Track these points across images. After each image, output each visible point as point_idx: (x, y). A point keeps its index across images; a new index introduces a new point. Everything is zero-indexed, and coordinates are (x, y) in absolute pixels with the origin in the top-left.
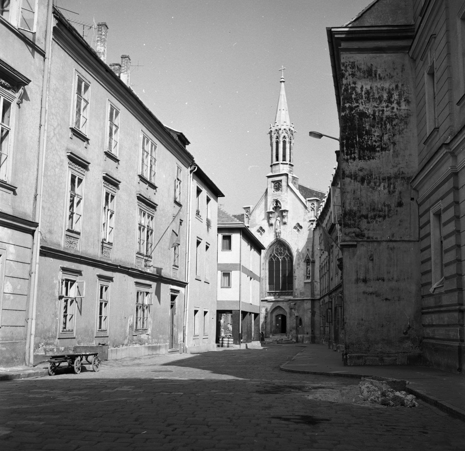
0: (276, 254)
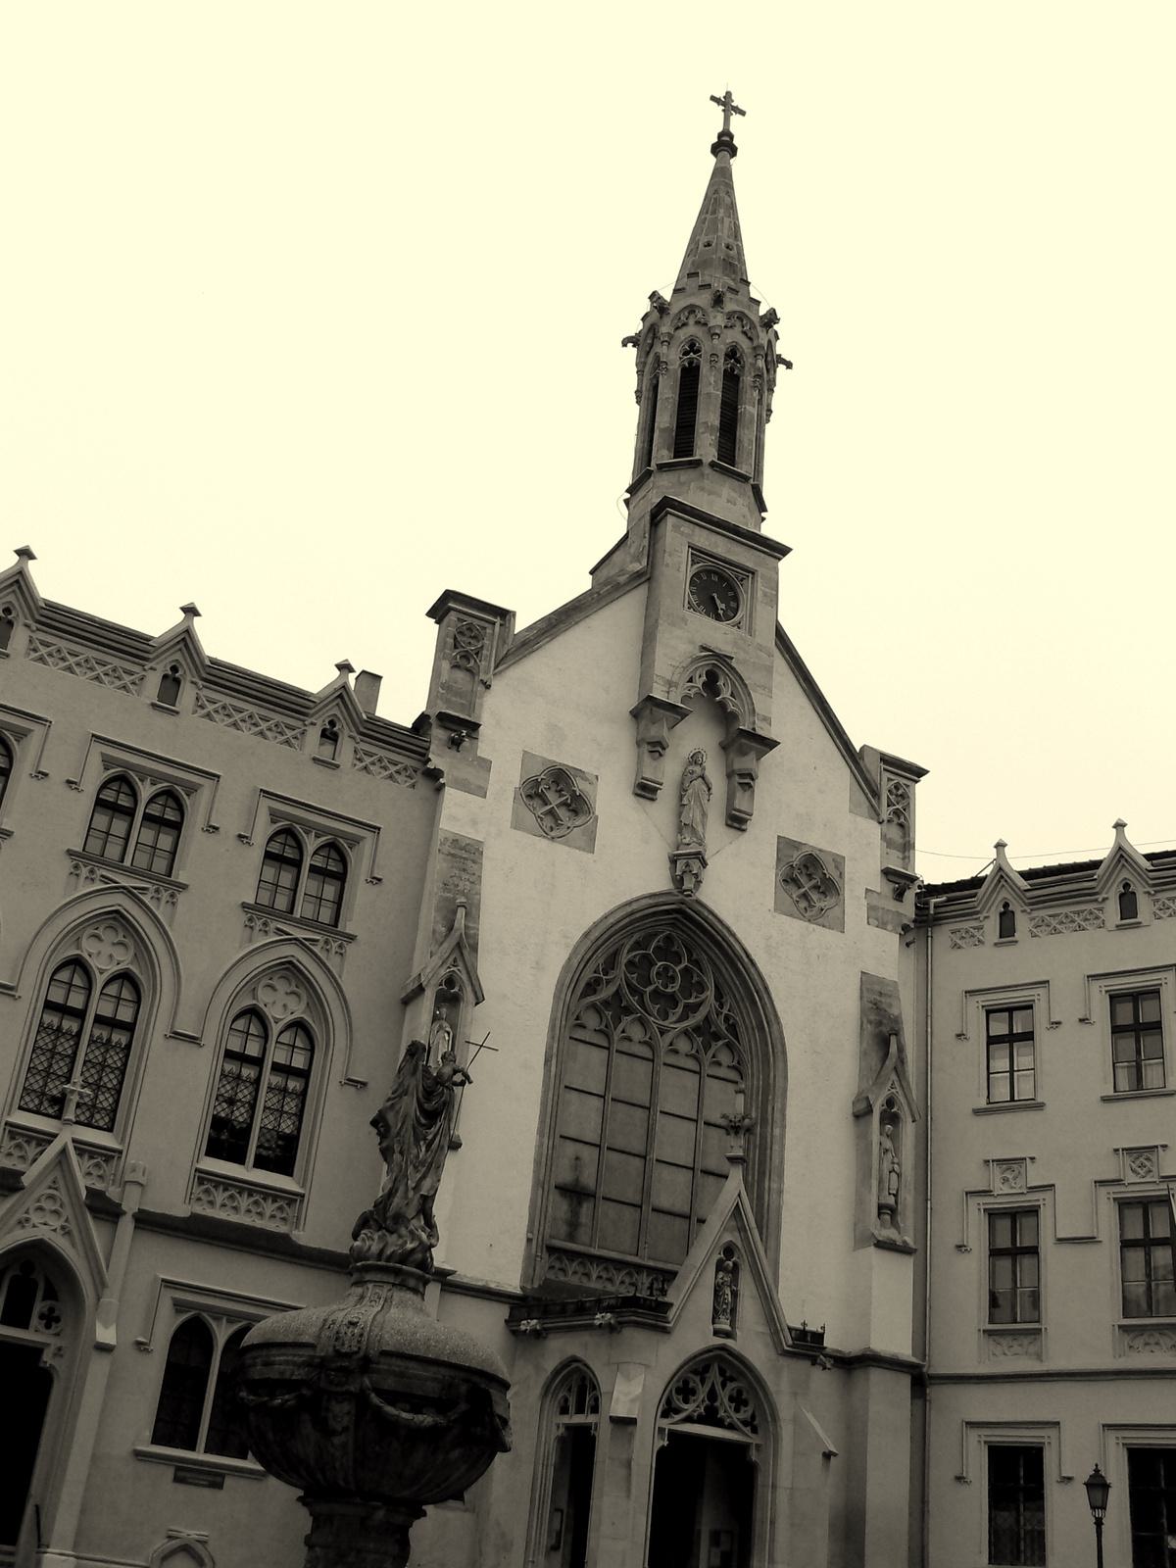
0: (634, 991)
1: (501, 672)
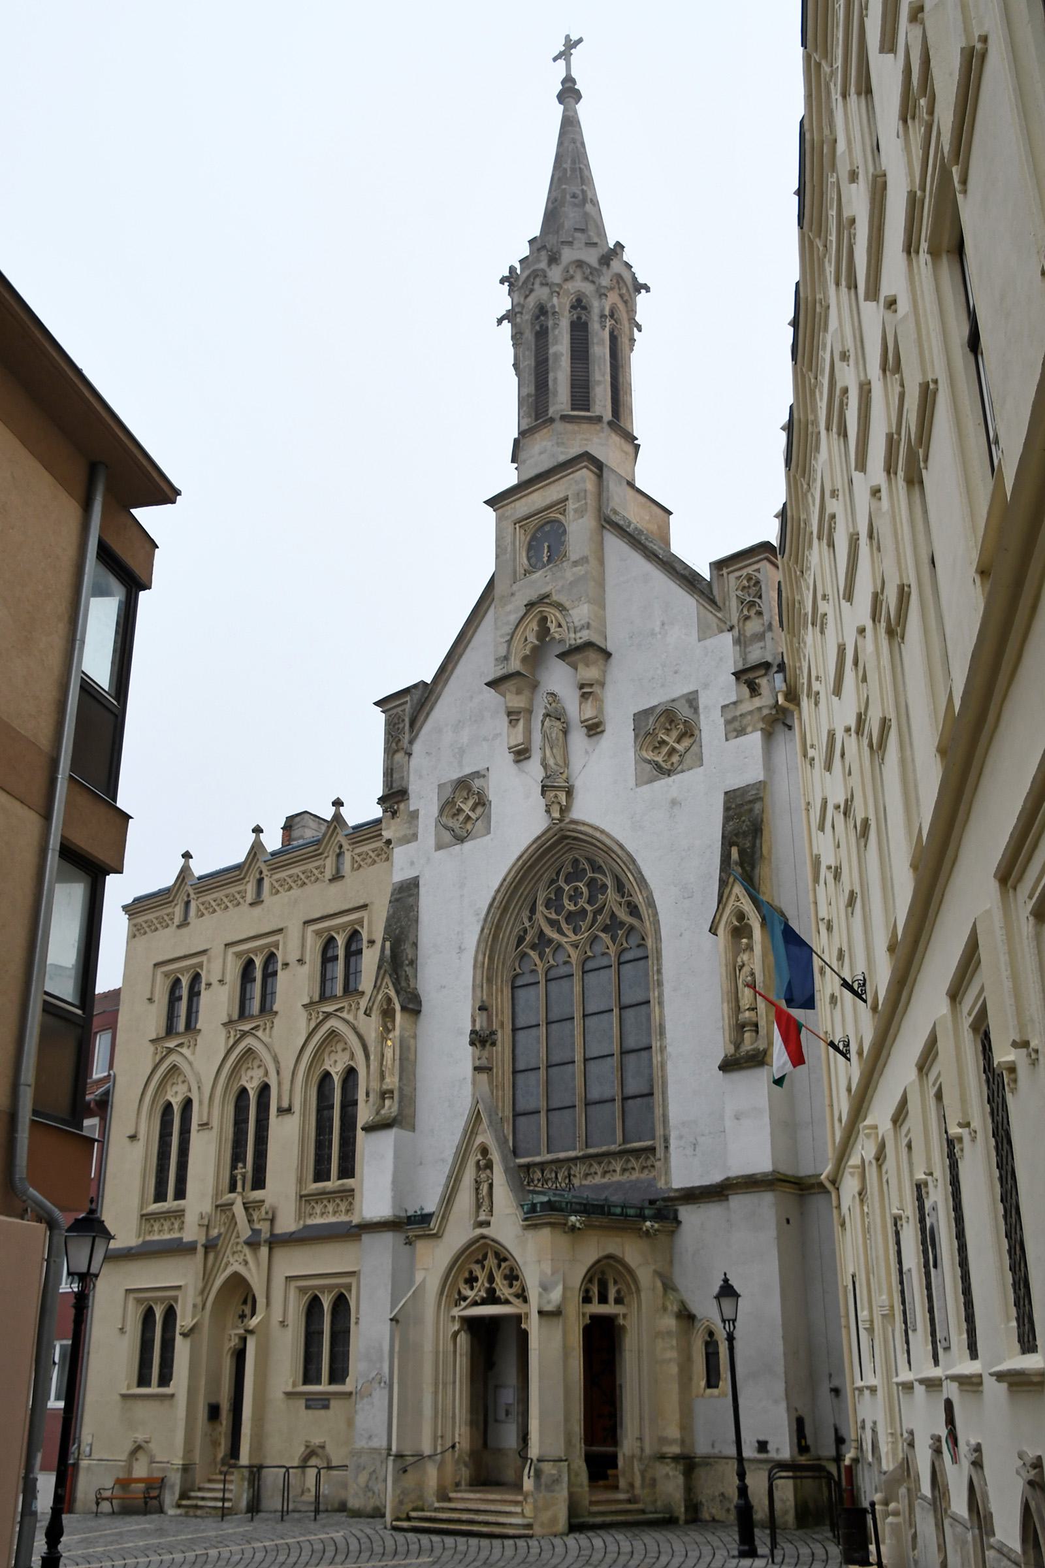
0: (553, 923)
1: (417, 735)
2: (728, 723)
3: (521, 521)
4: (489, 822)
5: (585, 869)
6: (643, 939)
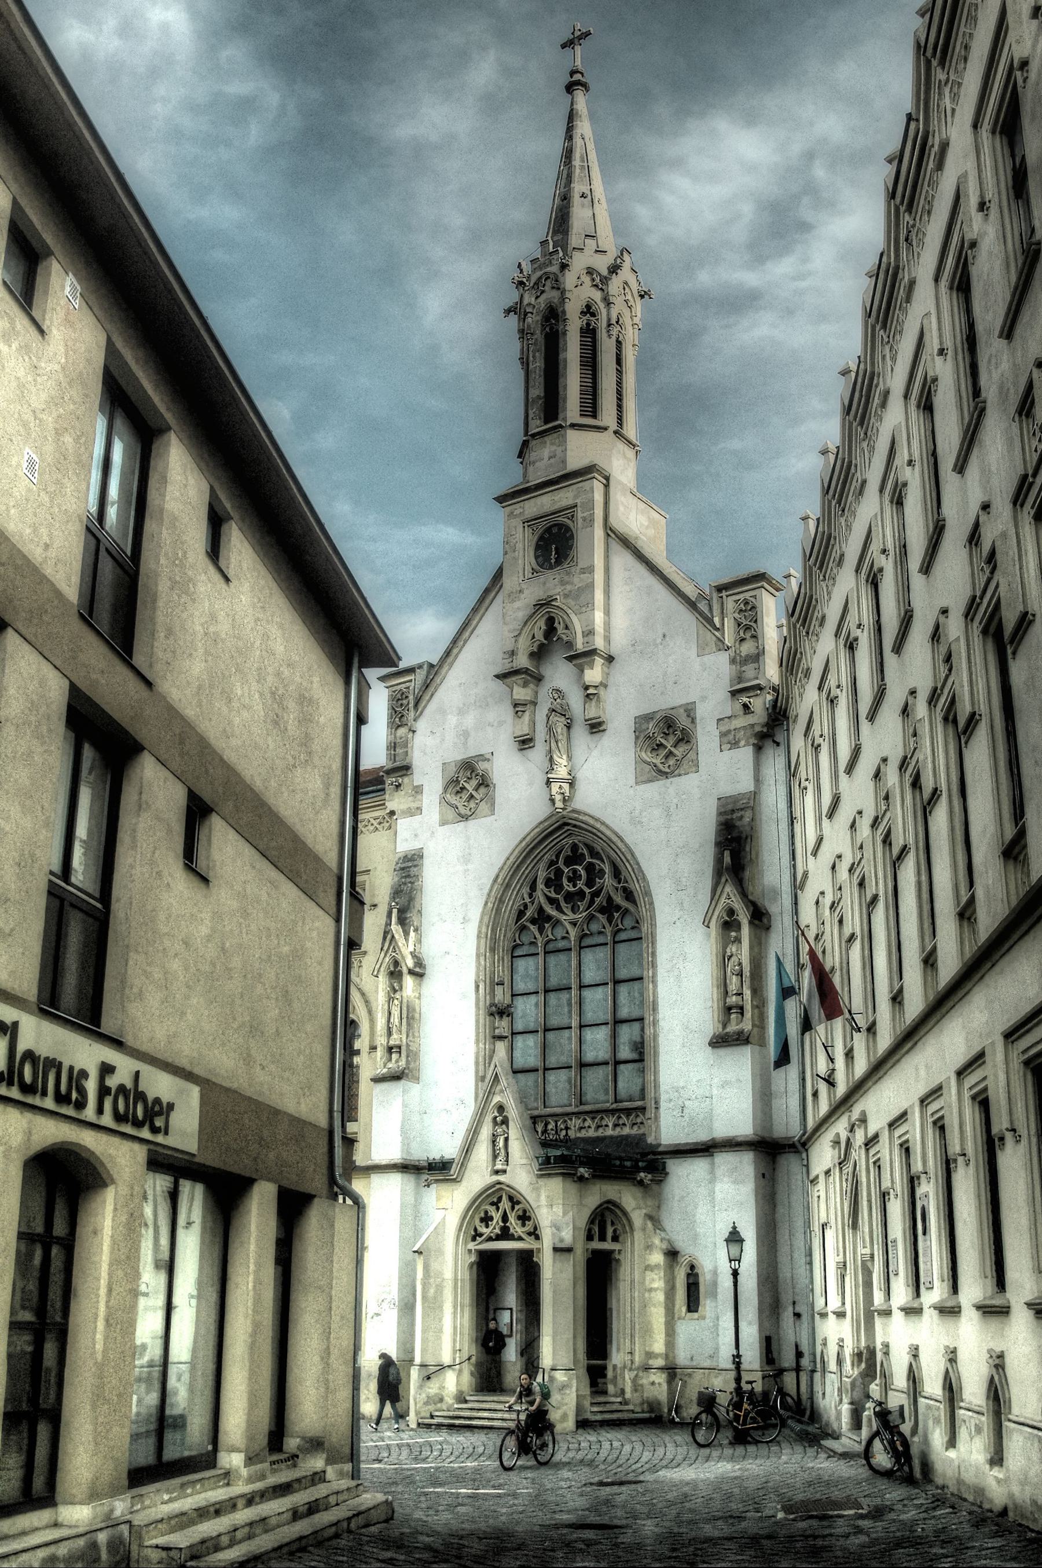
0: (551, 901)
1: (422, 713)
2: (723, 735)
3: (530, 522)
4: (493, 804)
5: (583, 855)
6: (637, 922)
